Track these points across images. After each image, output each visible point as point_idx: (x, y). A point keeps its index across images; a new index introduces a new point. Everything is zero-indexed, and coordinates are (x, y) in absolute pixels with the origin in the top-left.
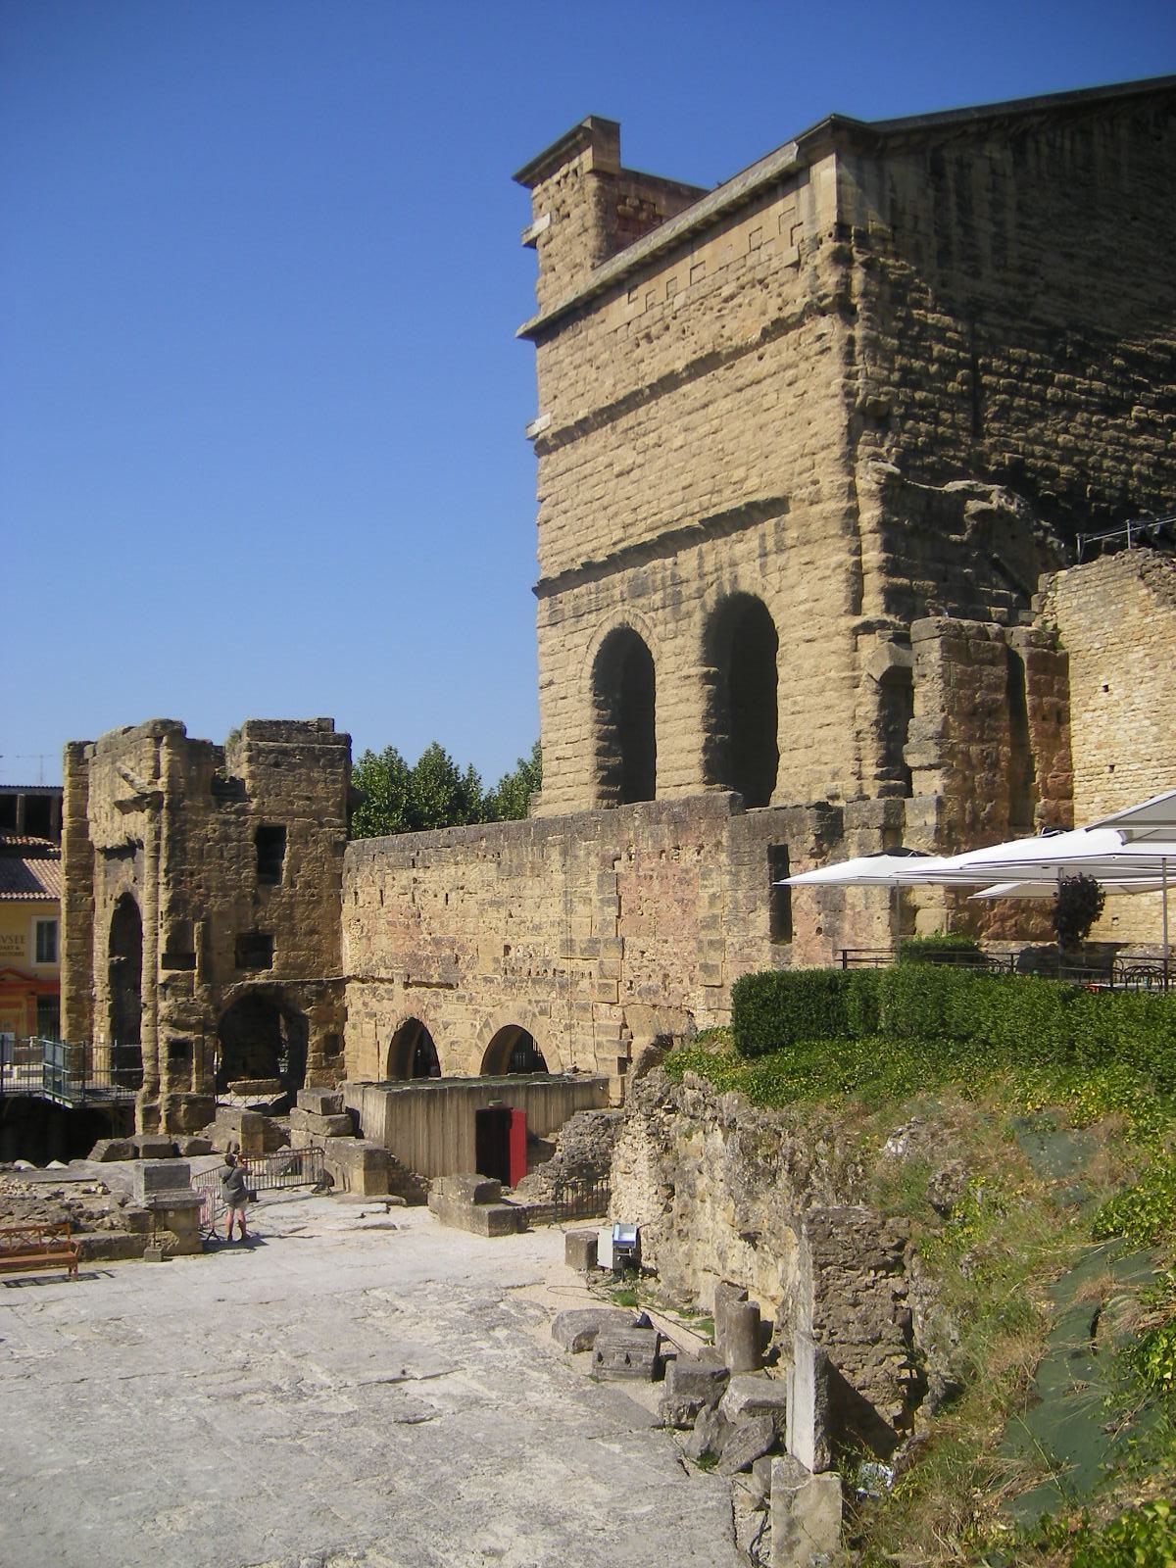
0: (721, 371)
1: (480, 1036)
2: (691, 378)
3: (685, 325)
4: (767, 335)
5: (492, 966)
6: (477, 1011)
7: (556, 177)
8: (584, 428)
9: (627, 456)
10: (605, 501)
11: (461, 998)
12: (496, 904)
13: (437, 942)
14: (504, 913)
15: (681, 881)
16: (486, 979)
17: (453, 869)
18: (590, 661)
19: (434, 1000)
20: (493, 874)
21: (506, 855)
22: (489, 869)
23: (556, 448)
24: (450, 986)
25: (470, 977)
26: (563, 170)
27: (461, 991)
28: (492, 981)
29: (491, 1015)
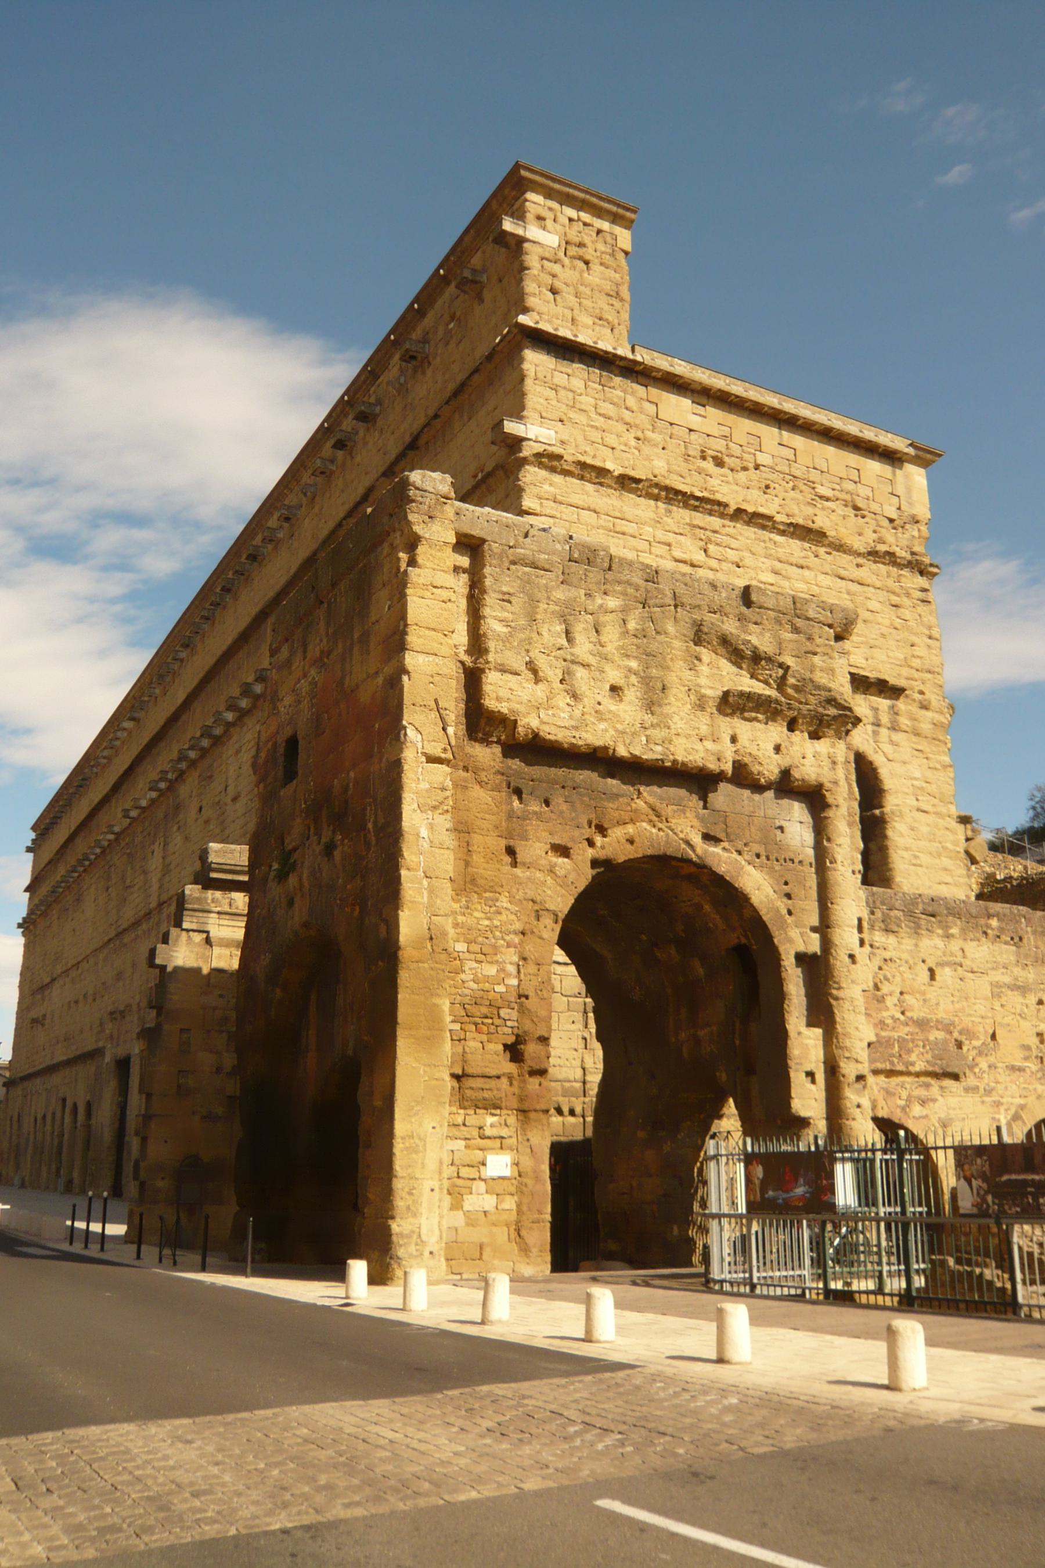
0: (822, 551)
2: (783, 533)
3: (772, 485)
4: (873, 555)
5: (1020, 1054)
6: (998, 1104)
8: (626, 483)
11: (967, 1090)
12: (1023, 989)
13: (922, 1024)
14: (1032, 999)
16: (1013, 1068)
17: (939, 943)
19: (922, 1092)
20: (1013, 958)
21: (1030, 939)
22: (1006, 953)
23: (566, 473)
24: (956, 1077)
25: (983, 1065)
27: (971, 1081)
28: (1021, 1069)
29: (1022, 1107)
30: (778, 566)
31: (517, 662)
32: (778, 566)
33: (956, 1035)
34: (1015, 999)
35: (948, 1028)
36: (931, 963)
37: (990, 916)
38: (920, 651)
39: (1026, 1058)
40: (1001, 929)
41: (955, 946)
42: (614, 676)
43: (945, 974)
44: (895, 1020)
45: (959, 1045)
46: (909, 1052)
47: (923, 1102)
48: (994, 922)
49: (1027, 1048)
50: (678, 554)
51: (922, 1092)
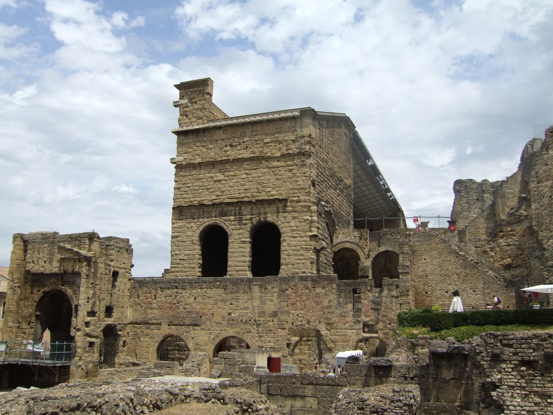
1: (214, 339)
7: (192, 90)
9: (221, 177)
10: (209, 187)
11: (201, 329)
13: (189, 312)
14: (228, 303)
15: (316, 297)
17: (199, 290)
18: (198, 232)
19: (187, 330)
22: (221, 291)
24: (198, 325)
26: (195, 89)
27: (203, 326)
29: (220, 334)
30: (247, 171)
31: (31, 261)
32: (247, 171)
33: (200, 314)
34: (220, 304)
35: (198, 313)
36: (195, 296)
37: (217, 281)
38: (299, 183)
39: (223, 321)
40: (220, 285)
41: (204, 291)
42: (45, 259)
43: (199, 299)
44: (182, 311)
45: (201, 317)
46: (185, 319)
47: (187, 332)
48: (218, 283)
49: (224, 317)
50: (215, 179)
51: (187, 330)
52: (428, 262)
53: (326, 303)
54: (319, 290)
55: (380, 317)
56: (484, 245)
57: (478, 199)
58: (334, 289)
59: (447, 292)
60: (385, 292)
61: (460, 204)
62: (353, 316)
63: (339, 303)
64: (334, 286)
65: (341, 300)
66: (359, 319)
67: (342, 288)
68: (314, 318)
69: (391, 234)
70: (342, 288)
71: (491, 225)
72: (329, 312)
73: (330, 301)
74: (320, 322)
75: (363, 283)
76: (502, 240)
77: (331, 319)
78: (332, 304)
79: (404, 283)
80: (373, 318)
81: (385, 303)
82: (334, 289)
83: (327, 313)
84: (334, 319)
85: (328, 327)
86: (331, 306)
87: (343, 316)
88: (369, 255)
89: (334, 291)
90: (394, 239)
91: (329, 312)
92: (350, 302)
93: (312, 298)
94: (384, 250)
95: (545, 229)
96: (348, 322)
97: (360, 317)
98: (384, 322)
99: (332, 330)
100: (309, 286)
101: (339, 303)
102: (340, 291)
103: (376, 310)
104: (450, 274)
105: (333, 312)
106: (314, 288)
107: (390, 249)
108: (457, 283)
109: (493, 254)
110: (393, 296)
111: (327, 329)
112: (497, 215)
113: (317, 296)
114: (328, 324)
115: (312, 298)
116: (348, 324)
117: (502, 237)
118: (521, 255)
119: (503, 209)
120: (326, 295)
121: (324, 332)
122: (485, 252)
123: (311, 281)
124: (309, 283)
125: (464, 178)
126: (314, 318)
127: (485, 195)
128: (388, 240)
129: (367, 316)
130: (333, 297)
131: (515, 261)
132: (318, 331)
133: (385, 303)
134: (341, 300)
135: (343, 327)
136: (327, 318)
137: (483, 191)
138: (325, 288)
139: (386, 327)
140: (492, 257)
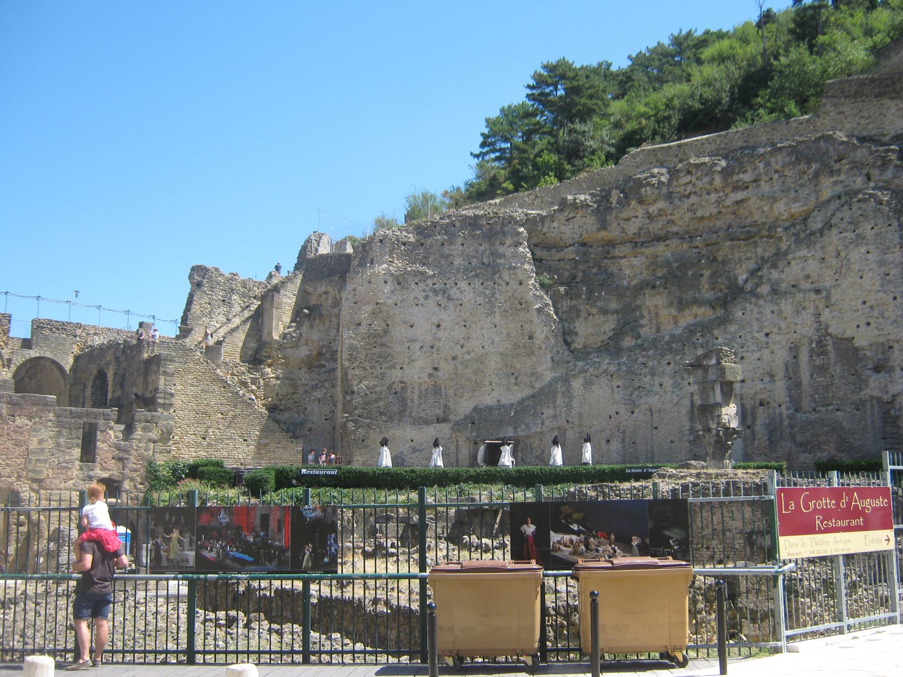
52: (179, 391)
53: (33, 444)
54: (20, 421)
55: (127, 471)
56: (244, 373)
57: (223, 301)
58: (50, 421)
59: (204, 439)
60: (138, 433)
61: (200, 304)
62: (81, 469)
63: (58, 445)
64: (51, 416)
65: (62, 440)
66: (91, 473)
67: (65, 420)
68: (8, 470)
69: (51, 330)
70: (65, 420)
71: (253, 345)
72: (38, 461)
73: (41, 442)
74: (19, 477)
75: (103, 414)
76: (269, 370)
77: (41, 472)
78: (45, 446)
79: (165, 420)
80: (115, 472)
81: (136, 450)
82: (50, 421)
83: (33, 462)
84: (46, 472)
85: (35, 486)
86: (43, 450)
87: (63, 468)
88: (10, 361)
89: (50, 424)
90: (56, 338)
91: (38, 461)
92: (78, 445)
93: (8, 434)
94: (38, 355)
95: (358, 367)
96: (72, 479)
97: (92, 470)
98: (132, 480)
99: (42, 492)
100: (4, 411)
101: (58, 445)
102: (60, 424)
103: (121, 460)
104: (210, 410)
105: (46, 461)
106: (13, 416)
107: (48, 355)
108: (221, 426)
109: (254, 387)
110: (150, 440)
111: (33, 490)
112: (265, 332)
113: (19, 430)
114: (35, 480)
115: (8, 434)
116: (71, 482)
117: (269, 366)
118: (293, 394)
119: (277, 325)
120: (36, 430)
121: (26, 493)
122: (244, 384)
123: (8, 403)
124: (4, 406)
125: (208, 265)
126: (8, 470)
127: (234, 297)
128: (46, 338)
129: (104, 469)
130: (47, 433)
131: (283, 402)
132: (16, 494)
133: (136, 450)
134: (62, 440)
135: (62, 485)
136: (34, 471)
137: (232, 290)
138: (32, 417)
139: (135, 487)
140: (252, 391)
